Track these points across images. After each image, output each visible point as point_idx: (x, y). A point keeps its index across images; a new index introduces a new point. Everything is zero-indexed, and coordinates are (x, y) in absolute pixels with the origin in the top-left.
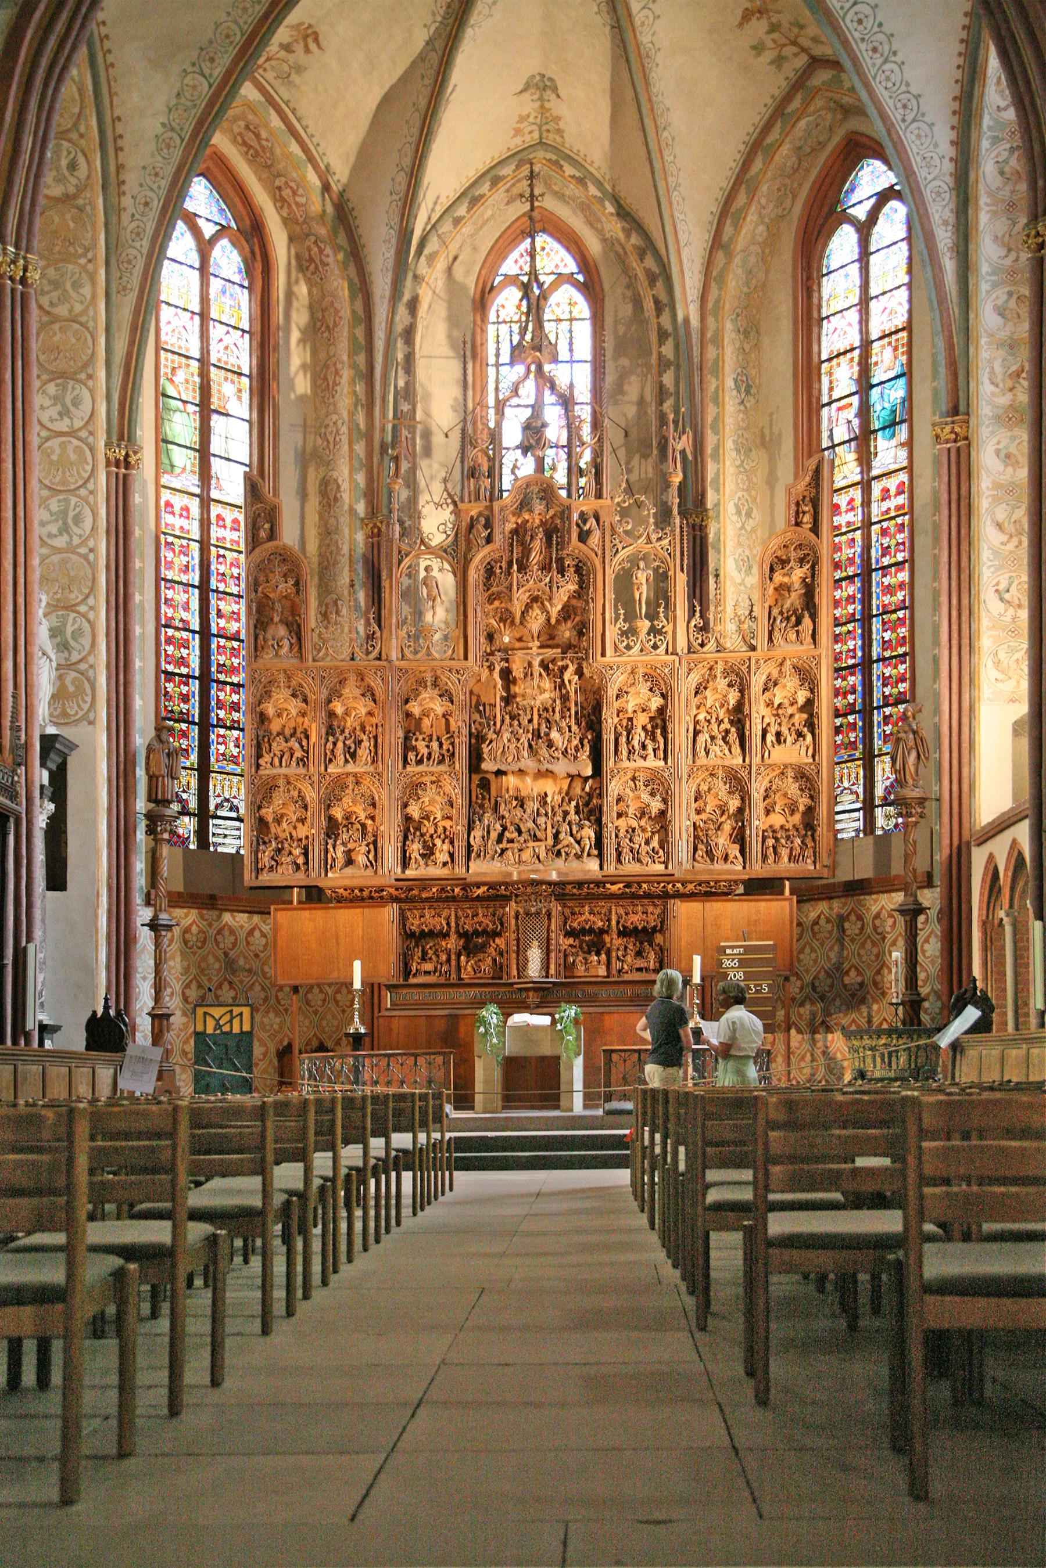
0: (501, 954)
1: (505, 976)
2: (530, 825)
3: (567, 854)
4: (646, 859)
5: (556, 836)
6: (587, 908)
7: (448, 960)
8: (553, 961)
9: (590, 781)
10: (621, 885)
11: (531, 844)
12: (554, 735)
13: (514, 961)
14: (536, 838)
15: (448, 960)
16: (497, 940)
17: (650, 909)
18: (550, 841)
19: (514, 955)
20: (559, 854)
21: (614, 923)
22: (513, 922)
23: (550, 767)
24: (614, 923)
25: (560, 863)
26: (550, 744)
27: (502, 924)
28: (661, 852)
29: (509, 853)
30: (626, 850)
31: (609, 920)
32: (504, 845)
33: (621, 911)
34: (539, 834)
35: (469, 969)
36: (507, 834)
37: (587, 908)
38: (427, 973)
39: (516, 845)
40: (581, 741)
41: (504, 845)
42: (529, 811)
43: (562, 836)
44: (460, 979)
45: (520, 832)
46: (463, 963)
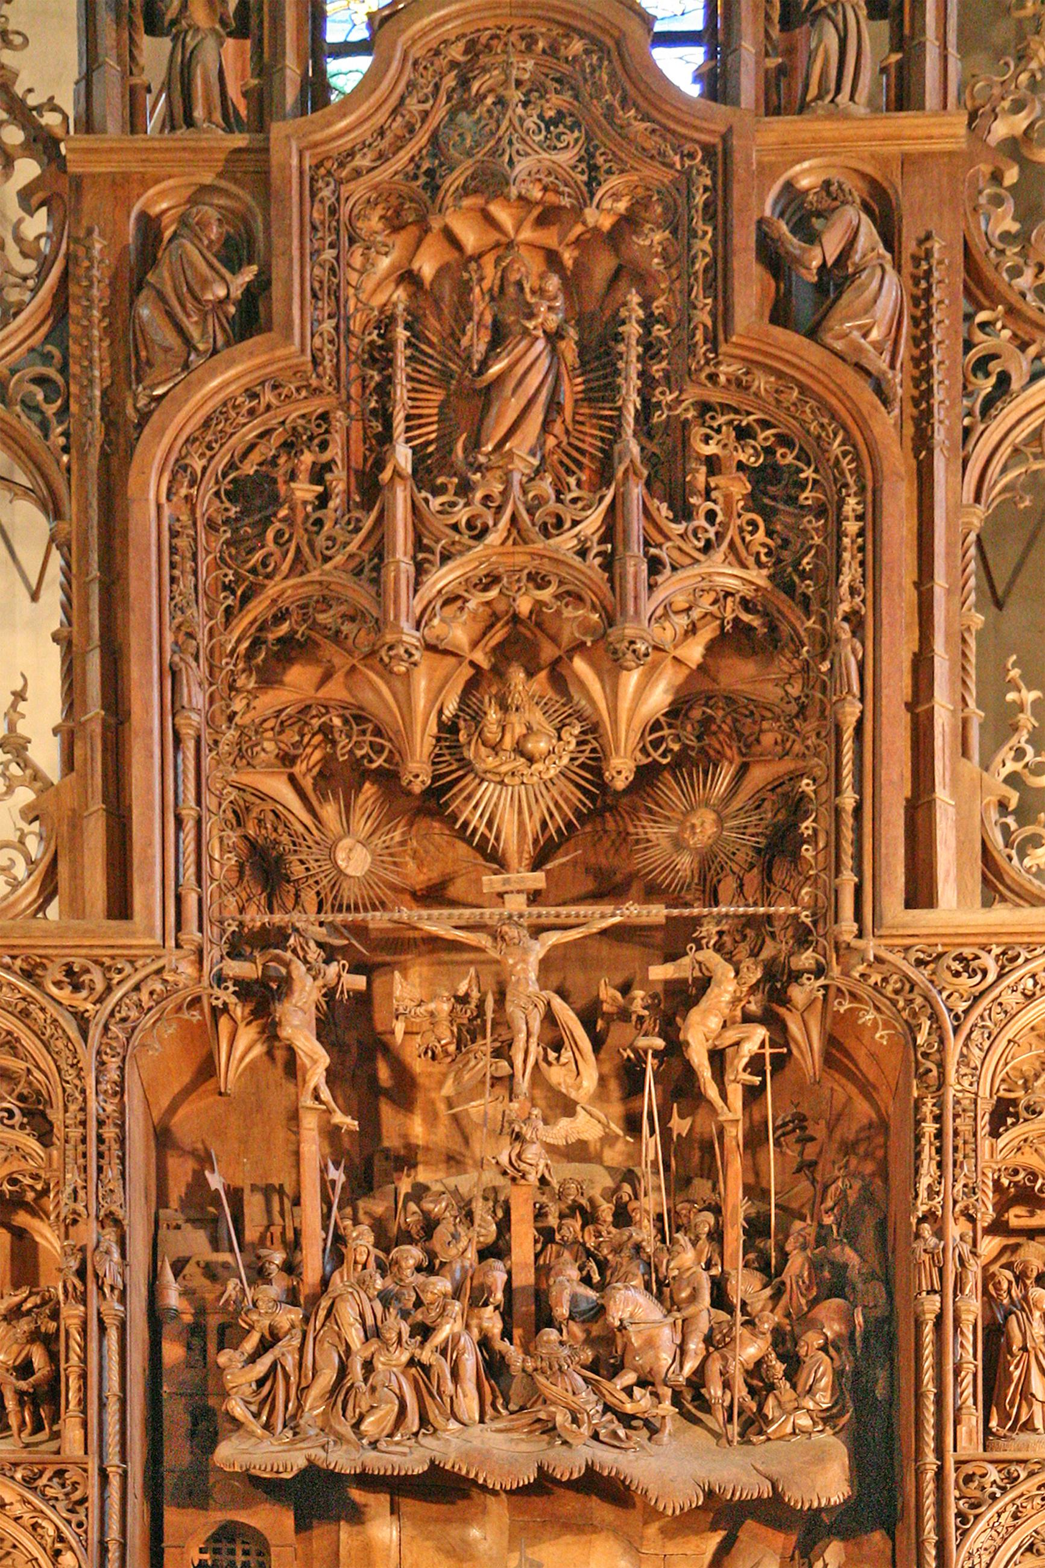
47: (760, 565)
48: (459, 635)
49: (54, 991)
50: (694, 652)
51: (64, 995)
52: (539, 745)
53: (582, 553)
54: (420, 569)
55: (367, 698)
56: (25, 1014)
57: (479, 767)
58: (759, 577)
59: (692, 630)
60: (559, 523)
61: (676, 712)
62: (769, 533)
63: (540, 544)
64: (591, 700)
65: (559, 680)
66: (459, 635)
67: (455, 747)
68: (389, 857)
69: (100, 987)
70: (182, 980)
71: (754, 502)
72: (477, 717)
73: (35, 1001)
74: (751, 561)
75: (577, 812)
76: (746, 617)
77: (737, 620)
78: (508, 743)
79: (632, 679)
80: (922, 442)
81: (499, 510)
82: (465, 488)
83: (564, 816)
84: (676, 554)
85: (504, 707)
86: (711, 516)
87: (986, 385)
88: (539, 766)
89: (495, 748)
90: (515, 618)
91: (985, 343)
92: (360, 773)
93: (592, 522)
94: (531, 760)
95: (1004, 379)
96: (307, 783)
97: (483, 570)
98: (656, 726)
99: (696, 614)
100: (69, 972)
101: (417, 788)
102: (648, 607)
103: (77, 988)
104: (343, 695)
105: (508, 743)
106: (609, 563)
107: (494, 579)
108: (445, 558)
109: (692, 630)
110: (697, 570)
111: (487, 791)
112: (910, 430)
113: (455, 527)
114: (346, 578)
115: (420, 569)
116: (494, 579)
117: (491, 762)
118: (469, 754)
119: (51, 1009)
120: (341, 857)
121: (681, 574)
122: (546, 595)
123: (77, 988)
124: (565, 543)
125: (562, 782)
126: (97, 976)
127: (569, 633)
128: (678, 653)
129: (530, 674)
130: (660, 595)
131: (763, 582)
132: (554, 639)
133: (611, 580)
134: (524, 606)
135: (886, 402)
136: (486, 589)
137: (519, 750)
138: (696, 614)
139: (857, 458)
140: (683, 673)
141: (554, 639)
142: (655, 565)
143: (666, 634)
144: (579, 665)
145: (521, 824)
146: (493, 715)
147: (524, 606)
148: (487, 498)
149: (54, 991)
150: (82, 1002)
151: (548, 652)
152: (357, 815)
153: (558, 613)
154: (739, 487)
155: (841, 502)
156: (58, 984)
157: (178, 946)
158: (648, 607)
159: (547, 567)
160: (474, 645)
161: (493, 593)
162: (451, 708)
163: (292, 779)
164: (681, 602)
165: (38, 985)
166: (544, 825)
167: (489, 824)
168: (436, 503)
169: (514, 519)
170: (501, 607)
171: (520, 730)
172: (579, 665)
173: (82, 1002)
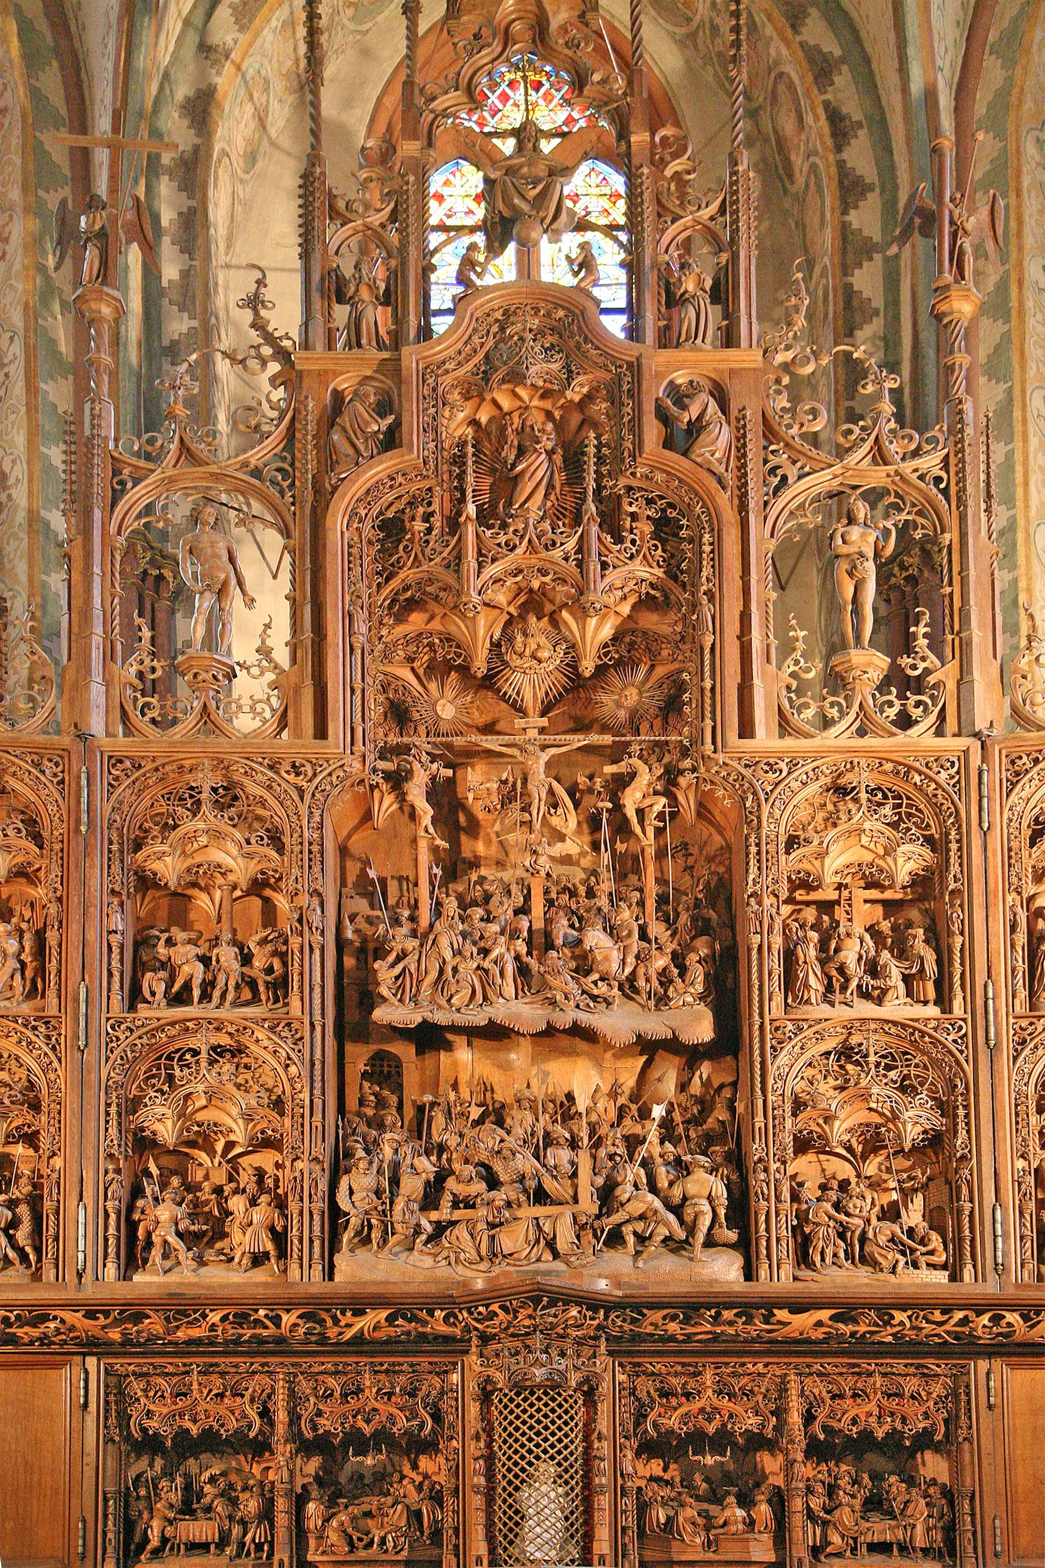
2: (525, 1162)
3: (641, 1239)
5: (607, 1195)
9: (705, 1069)
11: (528, 1212)
12: (596, 938)
14: (541, 1196)
18: (589, 1205)
20: (615, 1239)
23: (584, 1018)
26: (584, 965)
29: (461, 1232)
32: (444, 1213)
34: (550, 1185)
36: (451, 1183)
39: (482, 1212)
40: (678, 959)
41: (444, 1213)
42: (519, 1132)
43: (625, 1191)
45: (493, 1183)
47: (660, 566)
48: (502, 599)
49: (285, 775)
50: (626, 609)
51: (291, 778)
52: (544, 654)
53: (566, 559)
54: (481, 566)
55: (453, 629)
56: (269, 788)
57: (512, 664)
58: (659, 572)
59: (624, 598)
60: (554, 544)
61: (615, 639)
62: (664, 551)
63: (544, 554)
64: (572, 632)
65: (555, 622)
66: (502, 599)
67: (500, 655)
68: (466, 709)
69: (310, 773)
70: (354, 771)
71: (655, 535)
72: (511, 640)
73: (275, 781)
74: (654, 564)
75: (564, 687)
76: (653, 592)
77: (647, 593)
78: (527, 653)
79: (592, 622)
80: (743, 508)
81: (522, 537)
82: (504, 526)
83: (558, 690)
84: (615, 560)
85: (525, 634)
86: (633, 542)
87: (776, 481)
88: (544, 664)
89: (521, 655)
90: (531, 590)
91: (774, 461)
92: (448, 667)
93: (571, 544)
94: (540, 661)
95: (784, 479)
96: (421, 672)
97: (513, 567)
98: (606, 645)
99: (626, 590)
100: (294, 766)
101: (479, 675)
102: (601, 586)
103: (298, 774)
104: (440, 628)
105: (527, 653)
106: (580, 564)
107: (519, 571)
108: (494, 560)
109: (624, 598)
110: (627, 568)
111: (517, 677)
112: (736, 502)
113: (499, 545)
114: (440, 569)
115: (481, 566)
116: (519, 571)
117: (519, 662)
118: (507, 658)
119: (284, 785)
120: (439, 708)
121: (618, 570)
122: (547, 579)
123: (298, 774)
124: (557, 554)
125: (556, 673)
126: (308, 768)
127: (559, 599)
128: (617, 609)
129: (539, 619)
130: (607, 580)
131: (661, 575)
132: (552, 602)
133: (581, 572)
134: (536, 584)
135: (723, 488)
136: (515, 576)
137: (534, 656)
138: (626, 590)
139: (709, 515)
140: (619, 620)
141: (552, 602)
142: (604, 566)
143: (611, 599)
144: (565, 614)
145: (535, 694)
146: (519, 638)
147: (536, 584)
148: (516, 531)
149: (285, 775)
150: (301, 781)
151: (548, 608)
152: (447, 688)
153: (554, 588)
154: (648, 528)
155: (701, 537)
156: (287, 772)
157: (352, 753)
158: (601, 586)
159: (548, 565)
160: (509, 604)
161: (520, 578)
162: (497, 635)
163: (413, 669)
164: (618, 584)
165: (277, 773)
166: (547, 693)
167: (518, 693)
168: (488, 533)
169: (530, 541)
170: (523, 585)
171: (534, 646)
172: (565, 614)
173: (301, 781)
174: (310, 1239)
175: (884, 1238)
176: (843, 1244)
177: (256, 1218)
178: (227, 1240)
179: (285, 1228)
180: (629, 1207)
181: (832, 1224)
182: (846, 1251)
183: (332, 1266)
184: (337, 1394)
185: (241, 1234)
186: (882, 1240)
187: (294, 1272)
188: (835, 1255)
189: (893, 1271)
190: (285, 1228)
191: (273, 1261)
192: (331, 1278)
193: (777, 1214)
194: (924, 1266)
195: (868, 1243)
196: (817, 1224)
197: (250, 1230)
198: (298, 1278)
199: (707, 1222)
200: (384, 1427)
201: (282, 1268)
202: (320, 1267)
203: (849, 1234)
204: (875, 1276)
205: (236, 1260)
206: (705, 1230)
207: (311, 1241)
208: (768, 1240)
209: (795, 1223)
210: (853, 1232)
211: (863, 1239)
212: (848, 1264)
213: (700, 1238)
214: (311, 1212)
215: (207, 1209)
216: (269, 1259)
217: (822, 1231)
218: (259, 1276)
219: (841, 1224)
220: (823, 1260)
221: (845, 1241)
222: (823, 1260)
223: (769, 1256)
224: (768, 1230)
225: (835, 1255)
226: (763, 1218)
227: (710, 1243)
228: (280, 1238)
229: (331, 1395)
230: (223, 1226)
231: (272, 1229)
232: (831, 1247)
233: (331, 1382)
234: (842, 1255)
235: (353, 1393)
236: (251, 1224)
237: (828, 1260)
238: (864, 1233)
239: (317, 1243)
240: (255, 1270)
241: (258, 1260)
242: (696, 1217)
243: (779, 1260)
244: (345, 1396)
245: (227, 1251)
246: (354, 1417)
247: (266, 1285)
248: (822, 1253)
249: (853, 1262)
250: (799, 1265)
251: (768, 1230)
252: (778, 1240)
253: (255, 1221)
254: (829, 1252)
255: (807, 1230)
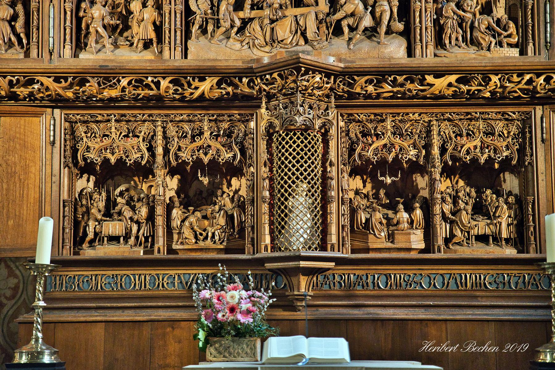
0: (241, 206)
1: (248, 247)
4: (486, 39)
6: (389, 124)
7: (151, 218)
8: (333, 219)
10: (452, 78)
13: (266, 219)
15: (151, 218)
16: (235, 182)
17: (499, 126)
19: (265, 208)
21: (436, 151)
22: (263, 145)
24: (436, 151)
25: (340, 44)
27: (243, 151)
28: (512, 25)
30: (450, 24)
31: (428, 147)
33: (448, 129)
35: (187, 233)
37: (389, 124)
38: (114, 239)
44: (171, 251)
46: (176, 223)
174: (175, 29)
175: (484, 27)
176: (461, 32)
177: (146, 16)
178: (130, 31)
179: (161, 22)
180: (346, 8)
181: (455, 17)
182: (463, 36)
183: (186, 49)
184: (189, 136)
185: (137, 27)
186: (483, 27)
187: (166, 53)
188: (457, 39)
189: (489, 49)
190: (161, 22)
191: (155, 45)
192: (186, 57)
193: (426, 11)
194: (506, 45)
195: (475, 30)
196: (447, 18)
197: (142, 24)
198: (168, 57)
199: (388, 18)
200: (214, 158)
201: (159, 50)
202: (180, 48)
203: (464, 24)
204: (479, 53)
205: (135, 45)
206: (386, 23)
207: (175, 32)
208: (421, 30)
209: (435, 17)
210: (467, 23)
211: (472, 27)
212: (463, 45)
213: (384, 28)
214: (175, 12)
215: (119, 10)
216: (152, 44)
217: (450, 21)
218: (148, 55)
219: (460, 18)
220: (450, 43)
221: (462, 29)
222: (450, 43)
223: (421, 40)
224: (420, 22)
225: (457, 39)
226: (417, 14)
227: (389, 32)
228: (158, 29)
229: (186, 136)
230: (128, 21)
231: (154, 23)
232: (455, 33)
233: (187, 127)
234: (460, 38)
235: (197, 135)
236: (143, 20)
237: (453, 42)
238: (473, 23)
239: (179, 33)
240: (145, 52)
241: (147, 45)
242: (381, 13)
243: (427, 43)
244: (193, 137)
245: (130, 38)
246: (198, 151)
247: (151, 61)
248: (450, 38)
249: (466, 44)
250: (437, 47)
251: (420, 22)
252: (426, 28)
253: (145, 18)
254: (454, 37)
255: (442, 22)
